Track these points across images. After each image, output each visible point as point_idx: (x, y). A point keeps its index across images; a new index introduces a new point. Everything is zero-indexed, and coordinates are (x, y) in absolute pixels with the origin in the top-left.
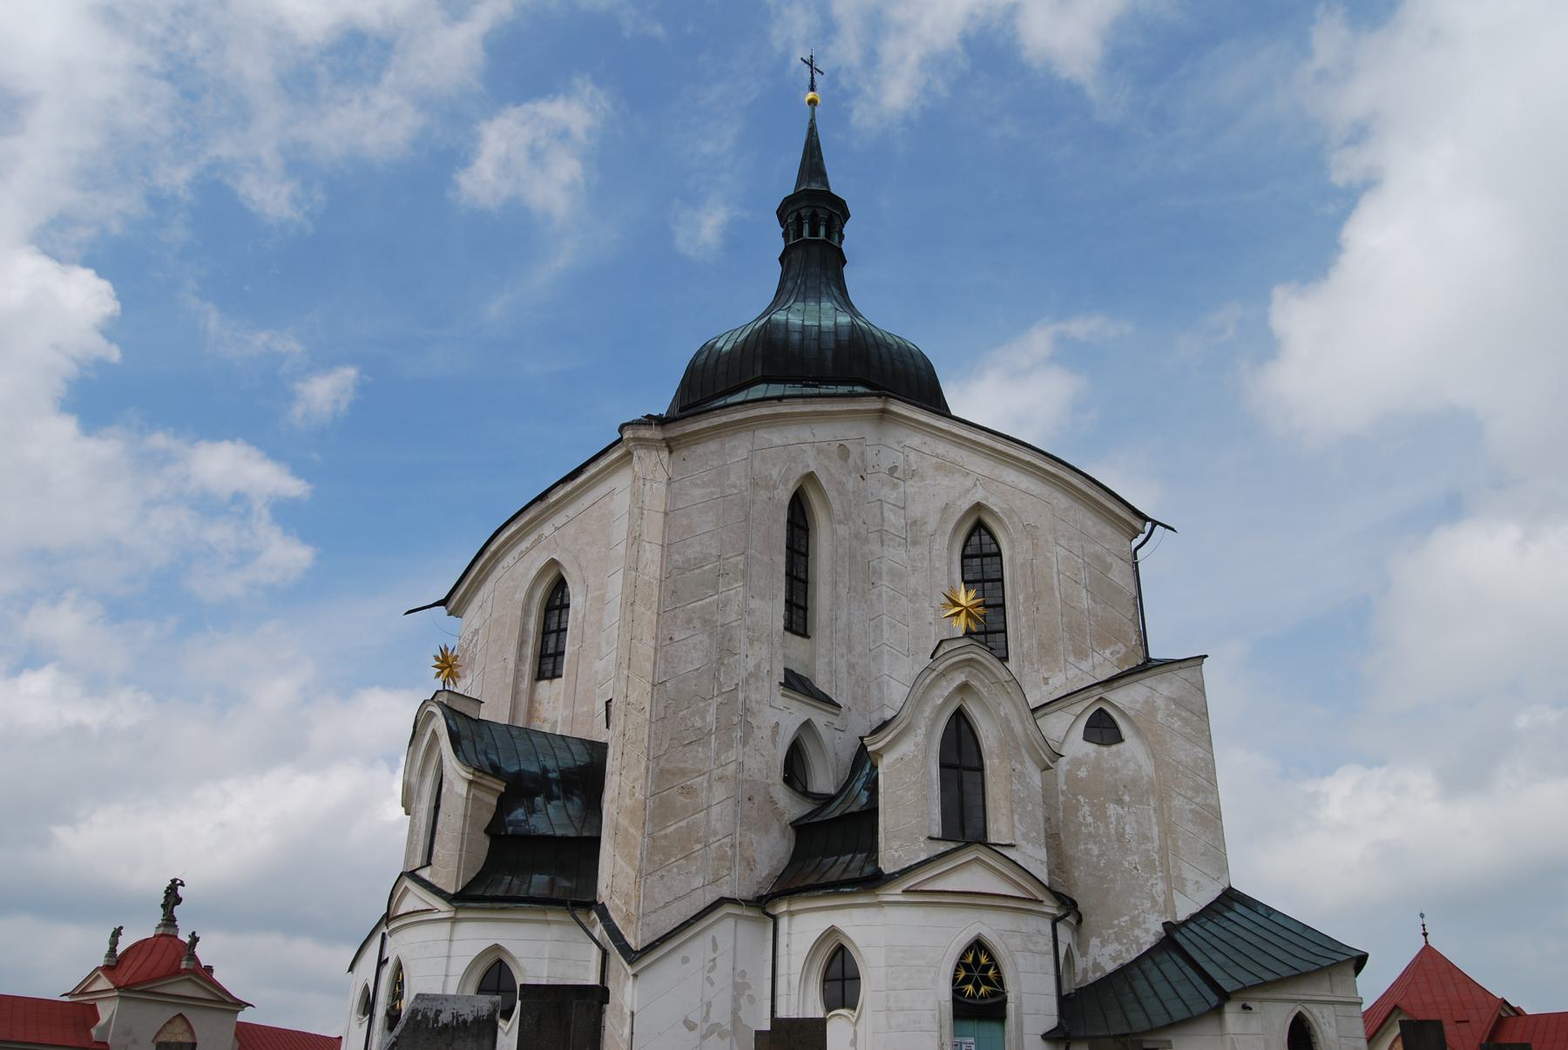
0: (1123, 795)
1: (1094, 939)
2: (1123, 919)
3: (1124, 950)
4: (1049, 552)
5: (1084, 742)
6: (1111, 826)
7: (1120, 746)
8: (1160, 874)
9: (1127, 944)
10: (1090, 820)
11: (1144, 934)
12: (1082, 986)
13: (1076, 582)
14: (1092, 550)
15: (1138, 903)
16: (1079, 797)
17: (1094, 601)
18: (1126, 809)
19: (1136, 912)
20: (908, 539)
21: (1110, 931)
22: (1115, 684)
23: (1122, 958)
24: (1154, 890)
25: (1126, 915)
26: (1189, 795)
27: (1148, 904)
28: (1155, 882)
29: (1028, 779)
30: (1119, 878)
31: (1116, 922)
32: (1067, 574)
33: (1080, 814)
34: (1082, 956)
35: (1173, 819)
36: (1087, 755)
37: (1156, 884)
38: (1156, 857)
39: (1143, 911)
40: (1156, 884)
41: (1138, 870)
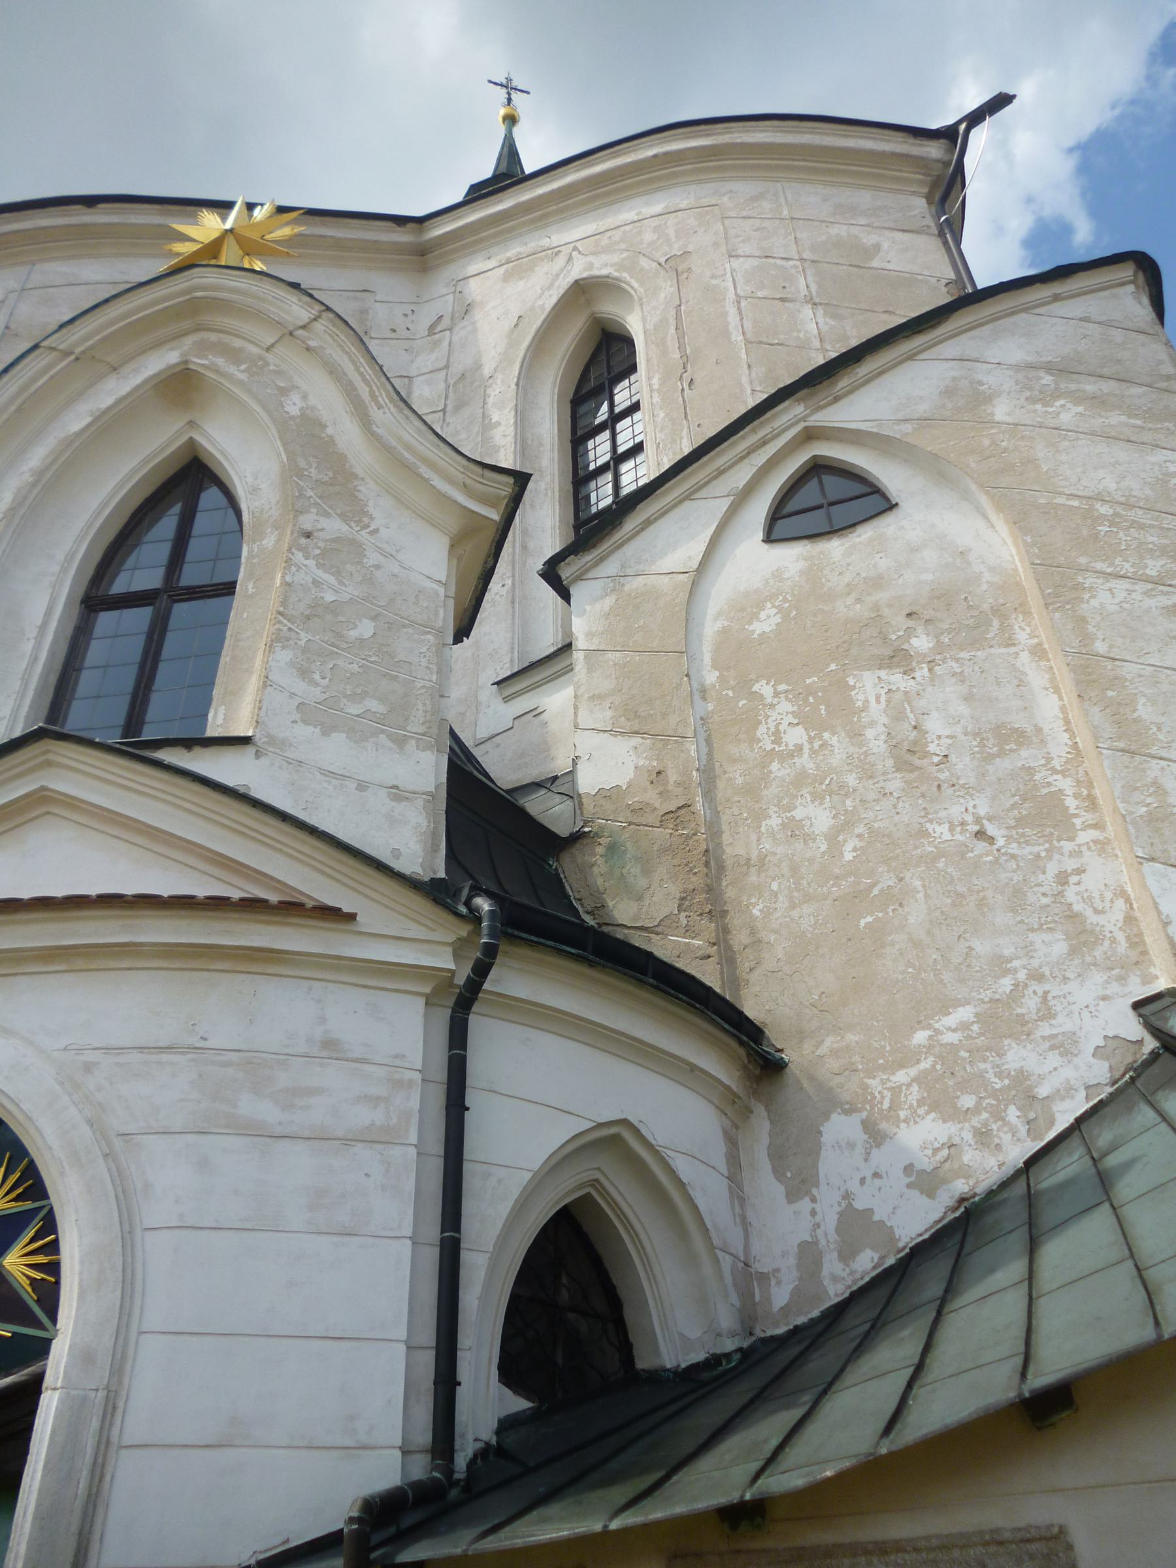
0: (910, 632)
1: (835, 1117)
2: (951, 1020)
3: (968, 1136)
4: (713, 277)
5: (766, 546)
6: (870, 733)
7: (887, 525)
8: (1084, 837)
9: (977, 1109)
10: (796, 736)
11: (1054, 1059)
12: (801, 1320)
13: (783, 300)
14: (824, 238)
15: (1007, 952)
16: (756, 688)
17: (835, 316)
18: (922, 672)
19: (1006, 984)
20: (449, 408)
21: (901, 1077)
22: (843, 383)
23: (965, 1172)
24: (1071, 894)
25: (957, 1003)
26: (1152, 572)
27: (1057, 946)
28: (1071, 865)
29: (373, 558)
30: (917, 883)
31: (920, 1037)
32: (760, 294)
33: (761, 731)
34: (793, 1196)
35: (1100, 647)
36: (778, 575)
37: (1080, 871)
38: (1066, 785)
39: (1038, 977)
40: (1080, 871)
41: (991, 840)
